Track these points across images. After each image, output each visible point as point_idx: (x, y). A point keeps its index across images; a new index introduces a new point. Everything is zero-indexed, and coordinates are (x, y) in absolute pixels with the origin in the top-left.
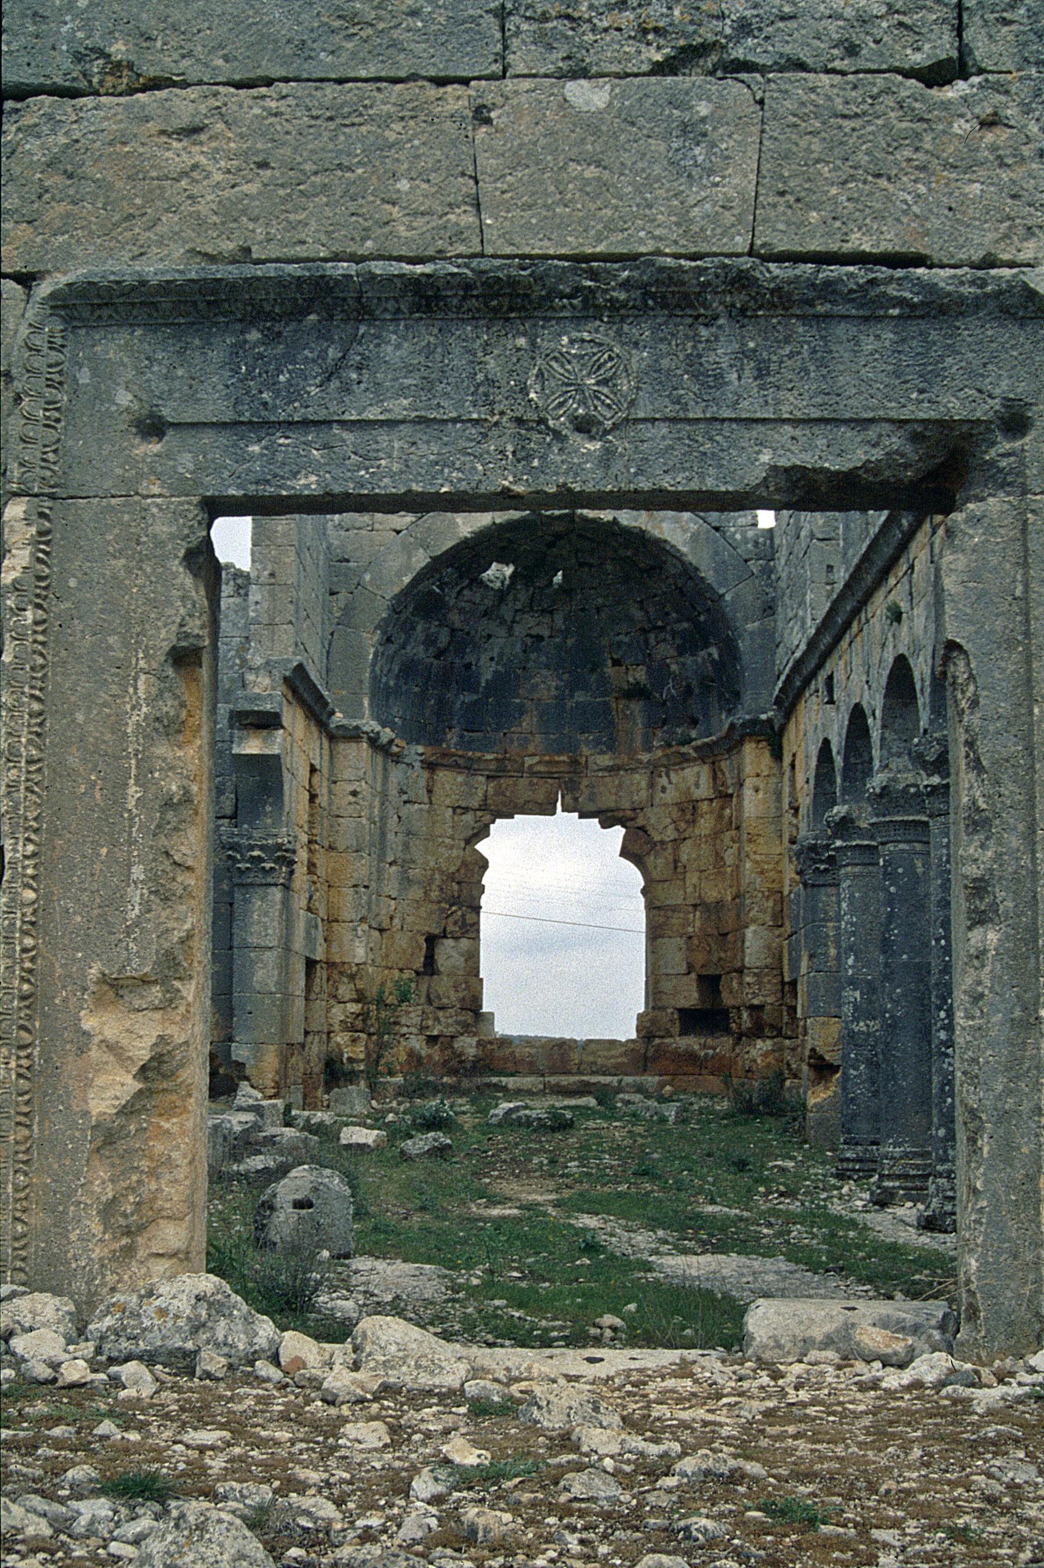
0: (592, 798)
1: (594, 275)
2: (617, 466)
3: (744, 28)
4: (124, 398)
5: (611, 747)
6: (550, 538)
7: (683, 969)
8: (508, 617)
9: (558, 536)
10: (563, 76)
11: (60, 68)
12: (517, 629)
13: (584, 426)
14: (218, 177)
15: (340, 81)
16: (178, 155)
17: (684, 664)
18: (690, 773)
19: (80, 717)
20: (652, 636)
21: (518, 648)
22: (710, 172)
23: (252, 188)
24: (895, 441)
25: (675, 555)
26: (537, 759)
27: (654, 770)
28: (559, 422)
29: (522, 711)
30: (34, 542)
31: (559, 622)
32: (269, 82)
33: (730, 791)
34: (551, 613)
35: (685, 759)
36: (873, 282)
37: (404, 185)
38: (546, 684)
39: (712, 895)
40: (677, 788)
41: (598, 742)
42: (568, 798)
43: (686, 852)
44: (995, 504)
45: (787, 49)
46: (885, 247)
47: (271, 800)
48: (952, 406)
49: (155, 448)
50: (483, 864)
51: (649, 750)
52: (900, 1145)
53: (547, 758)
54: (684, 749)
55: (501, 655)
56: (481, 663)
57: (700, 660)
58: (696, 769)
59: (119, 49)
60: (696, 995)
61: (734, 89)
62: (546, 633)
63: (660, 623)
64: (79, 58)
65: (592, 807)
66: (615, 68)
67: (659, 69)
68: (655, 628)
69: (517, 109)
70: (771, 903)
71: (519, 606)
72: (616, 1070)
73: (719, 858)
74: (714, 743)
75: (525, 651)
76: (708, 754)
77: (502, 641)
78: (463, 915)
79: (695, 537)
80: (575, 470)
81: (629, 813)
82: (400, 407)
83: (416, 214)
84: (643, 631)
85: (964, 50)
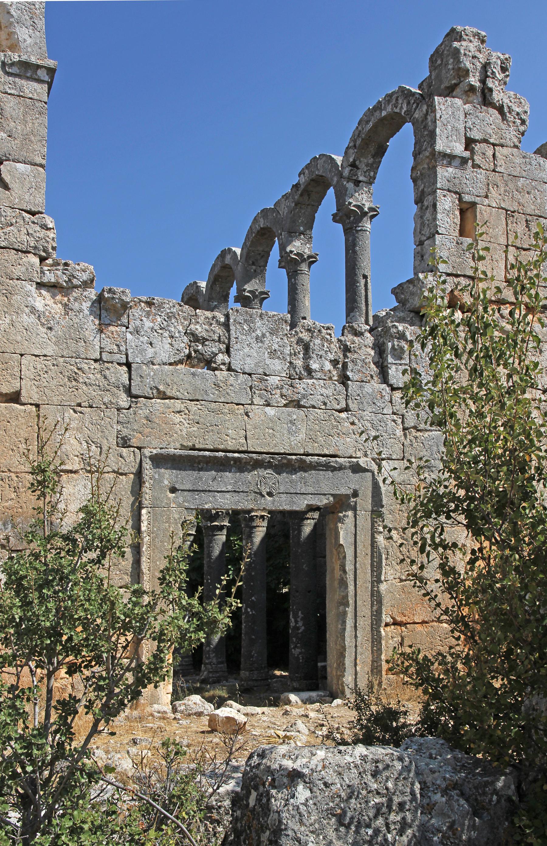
1: (273, 458)
2: (276, 503)
3: (304, 396)
4: (166, 482)
10: (264, 405)
11: (148, 392)
13: (270, 494)
14: (186, 425)
15: (215, 402)
16: (178, 418)
19: (158, 563)
22: (296, 433)
23: (195, 429)
24: (331, 499)
28: (264, 493)
30: (148, 519)
32: (198, 400)
36: (330, 462)
37: (230, 431)
44: (350, 513)
45: (312, 403)
46: (331, 453)
48: (344, 491)
49: (174, 495)
59: (161, 388)
61: (301, 413)
64: (151, 389)
66: (276, 405)
67: (285, 406)
69: (255, 414)
80: (266, 504)
82: (230, 488)
83: (232, 439)
85: (347, 405)
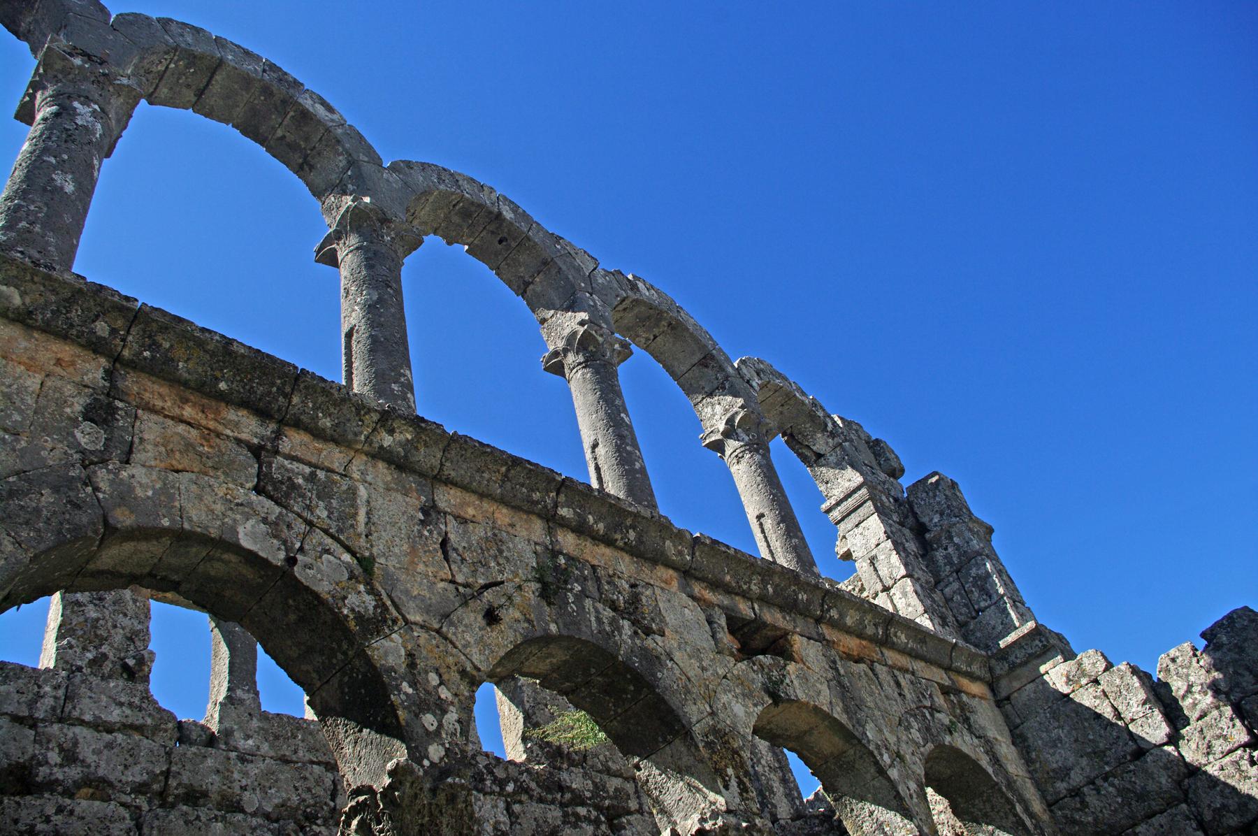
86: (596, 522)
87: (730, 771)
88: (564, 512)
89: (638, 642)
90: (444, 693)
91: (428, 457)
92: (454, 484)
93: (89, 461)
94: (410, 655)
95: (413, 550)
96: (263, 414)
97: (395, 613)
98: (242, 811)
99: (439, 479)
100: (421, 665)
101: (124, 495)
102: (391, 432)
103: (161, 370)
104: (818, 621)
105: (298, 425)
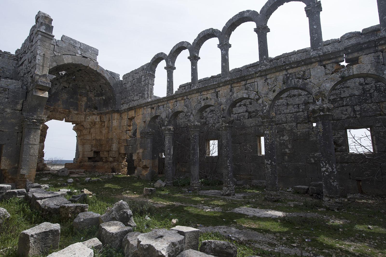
0: (72, 119)
5: (77, 110)
6: (78, 70)
7: (90, 150)
8: (61, 82)
9: (80, 70)
12: (62, 84)
17: (95, 98)
18: (94, 117)
20: (89, 93)
21: (61, 88)
25: (106, 79)
26: (62, 110)
27: (86, 116)
29: (59, 100)
31: (71, 85)
33: (105, 121)
34: (70, 83)
35: (94, 114)
38: (65, 96)
39: (98, 138)
40: (91, 119)
41: (74, 109)
42: (67, 118)
43: (92, 130)
47: (40, 108)
50: (47, 128)
51: (85, 112)
52: (197, 181)
53: (64, 110)
54: (94, 113)
55: (57, 88)
56: (53, 89)
57: (99, 98)
58: (96, 116)
60: (93, 155)
62: (67, 87)
63: (92, 91)
65: (71, 120)
68: (91, 91)
70: (118, 140)
71: (64, 80)
72: (75, 169)
73: (101, 132)
74: (103, 112)
75: (62, 89)
76: (100, 114)
77: (58, 86)
78: (43, 138)
79: (110, 78)
81: (79, 122)
84: (88, 91)
86: (294, 66)
87: (320, 98)
88: (287, 68)
89: (303, 82)
90: (267, 104)
91: (263, 74)
92: (268, 74)
93: (231, 96)
94: (262, 101)
95: (263, 87)
96: (244, 80)
97: (261, 96)
98: (302, 95)
99: (266, 75)
100: (264, 102)
101: (234, 98)
102: (257, 74)
103: (234, 83)
104: (376, 46)
105: (248, 79)
